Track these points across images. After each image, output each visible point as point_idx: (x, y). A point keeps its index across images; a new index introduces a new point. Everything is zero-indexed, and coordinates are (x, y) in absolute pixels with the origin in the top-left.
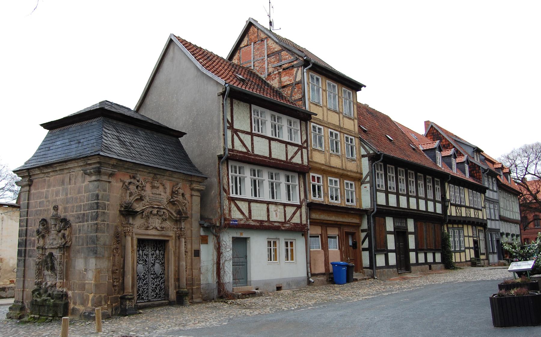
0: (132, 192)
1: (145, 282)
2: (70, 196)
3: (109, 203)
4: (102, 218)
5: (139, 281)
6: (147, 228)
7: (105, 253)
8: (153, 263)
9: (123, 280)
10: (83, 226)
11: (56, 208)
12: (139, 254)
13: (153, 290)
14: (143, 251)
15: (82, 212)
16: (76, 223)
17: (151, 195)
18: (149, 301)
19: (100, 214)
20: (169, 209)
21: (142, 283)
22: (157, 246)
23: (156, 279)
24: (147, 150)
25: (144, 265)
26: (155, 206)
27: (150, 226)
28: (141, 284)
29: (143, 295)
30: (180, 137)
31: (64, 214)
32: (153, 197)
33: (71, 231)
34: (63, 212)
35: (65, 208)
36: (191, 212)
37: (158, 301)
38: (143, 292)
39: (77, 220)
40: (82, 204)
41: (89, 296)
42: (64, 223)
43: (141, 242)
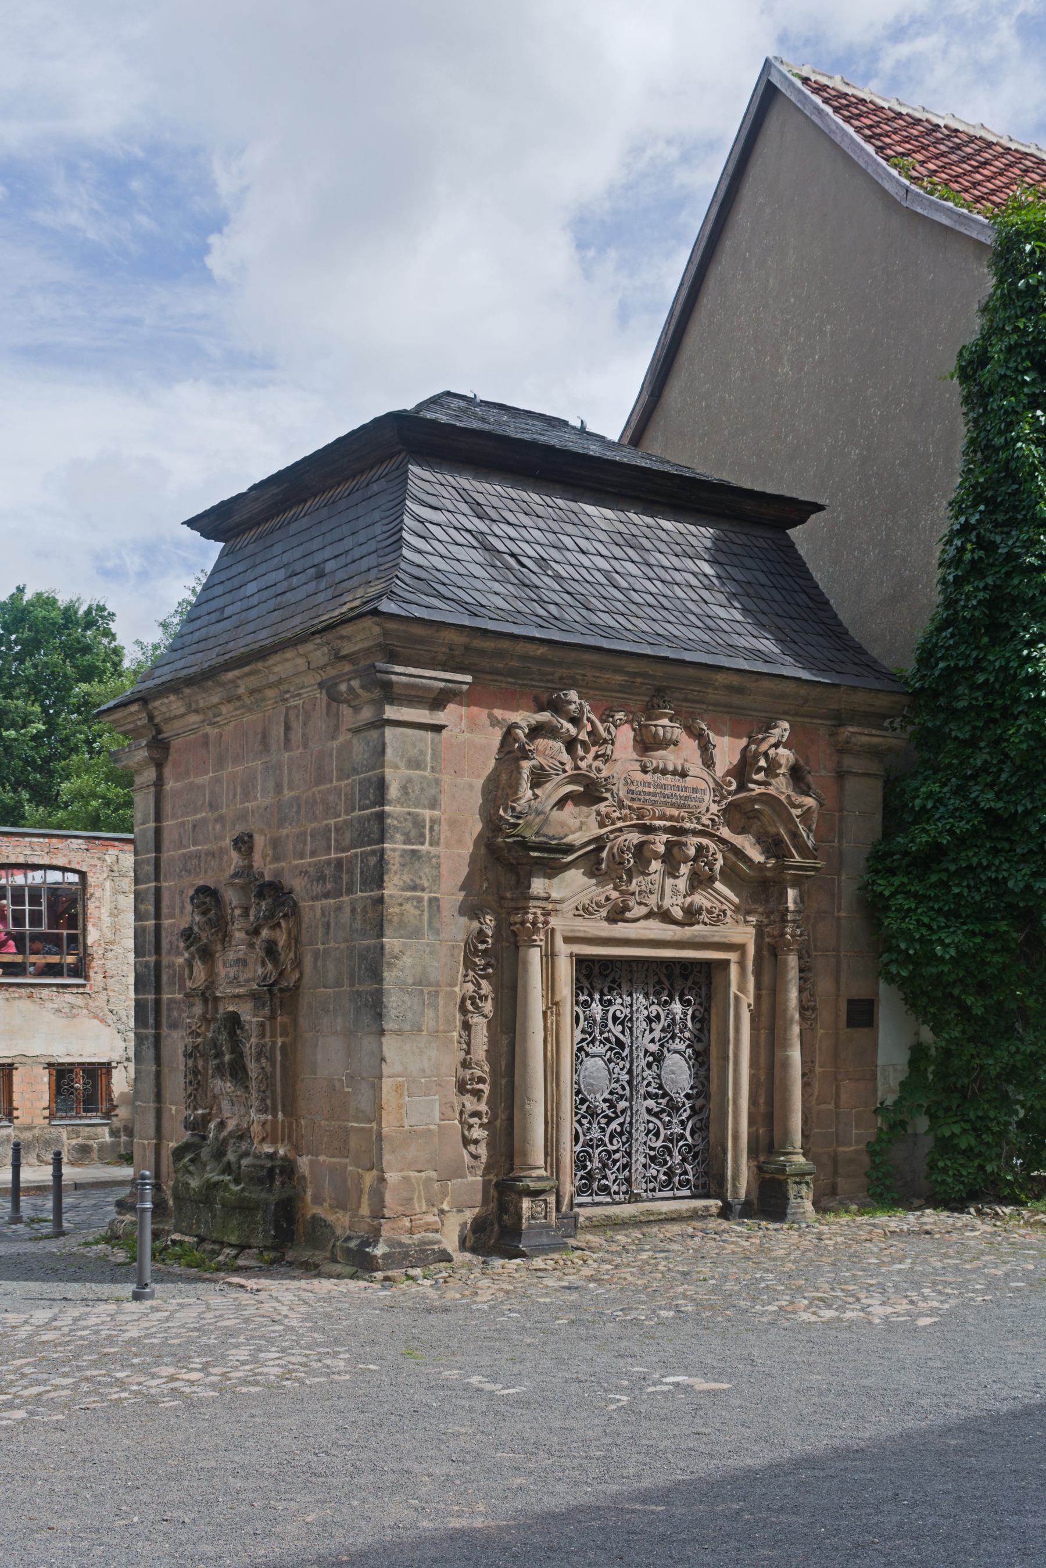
0: (542, 768)
1: (614, 1125)
2: (292, 794)
3: (436, 813)
4: (406, 878)
5: (590, 1123)
6: (617, 915)
7: (422, 1013)
8: (652, 1054)
9: (511, 1119)
10: (339, 908)
11: (244, 843)
12: (591, 1020)
13: (653, 1159)
14: (606, 1004)
15: (333, 856)
16: (313, 899)
17: (639, 776)
18: (635, 1198)
19: (397, 859)
20: (725, 832)
21: (603, 1130)
22: (672, 985)
23: (669, 1115)
24: (624, 584)
25: (610, 1061)
26: (662, 823)
27: (631, 903)
28: (596, 1134)
29: (605, 1177)
30: (794, 525)
31: (272, 867)
32: (648, 784)
33: (299, 932)
34: (268, 859)
35: (275, 843)
36: (836, 844)
37: (675, 1198)
38: (605, 1165)
39: (318, 889)
40: (332, 822)
41: (360, 1177)
42: (270, 900)
43: (596, 971)
